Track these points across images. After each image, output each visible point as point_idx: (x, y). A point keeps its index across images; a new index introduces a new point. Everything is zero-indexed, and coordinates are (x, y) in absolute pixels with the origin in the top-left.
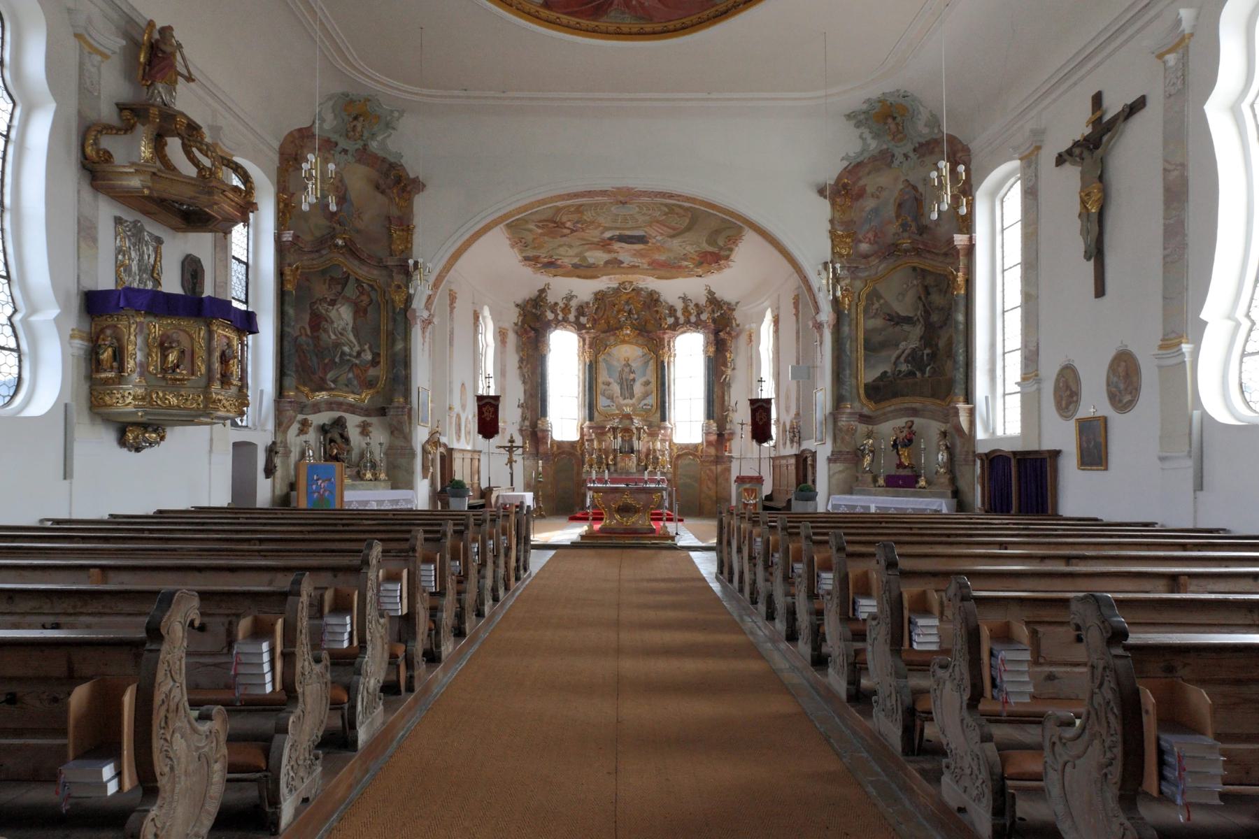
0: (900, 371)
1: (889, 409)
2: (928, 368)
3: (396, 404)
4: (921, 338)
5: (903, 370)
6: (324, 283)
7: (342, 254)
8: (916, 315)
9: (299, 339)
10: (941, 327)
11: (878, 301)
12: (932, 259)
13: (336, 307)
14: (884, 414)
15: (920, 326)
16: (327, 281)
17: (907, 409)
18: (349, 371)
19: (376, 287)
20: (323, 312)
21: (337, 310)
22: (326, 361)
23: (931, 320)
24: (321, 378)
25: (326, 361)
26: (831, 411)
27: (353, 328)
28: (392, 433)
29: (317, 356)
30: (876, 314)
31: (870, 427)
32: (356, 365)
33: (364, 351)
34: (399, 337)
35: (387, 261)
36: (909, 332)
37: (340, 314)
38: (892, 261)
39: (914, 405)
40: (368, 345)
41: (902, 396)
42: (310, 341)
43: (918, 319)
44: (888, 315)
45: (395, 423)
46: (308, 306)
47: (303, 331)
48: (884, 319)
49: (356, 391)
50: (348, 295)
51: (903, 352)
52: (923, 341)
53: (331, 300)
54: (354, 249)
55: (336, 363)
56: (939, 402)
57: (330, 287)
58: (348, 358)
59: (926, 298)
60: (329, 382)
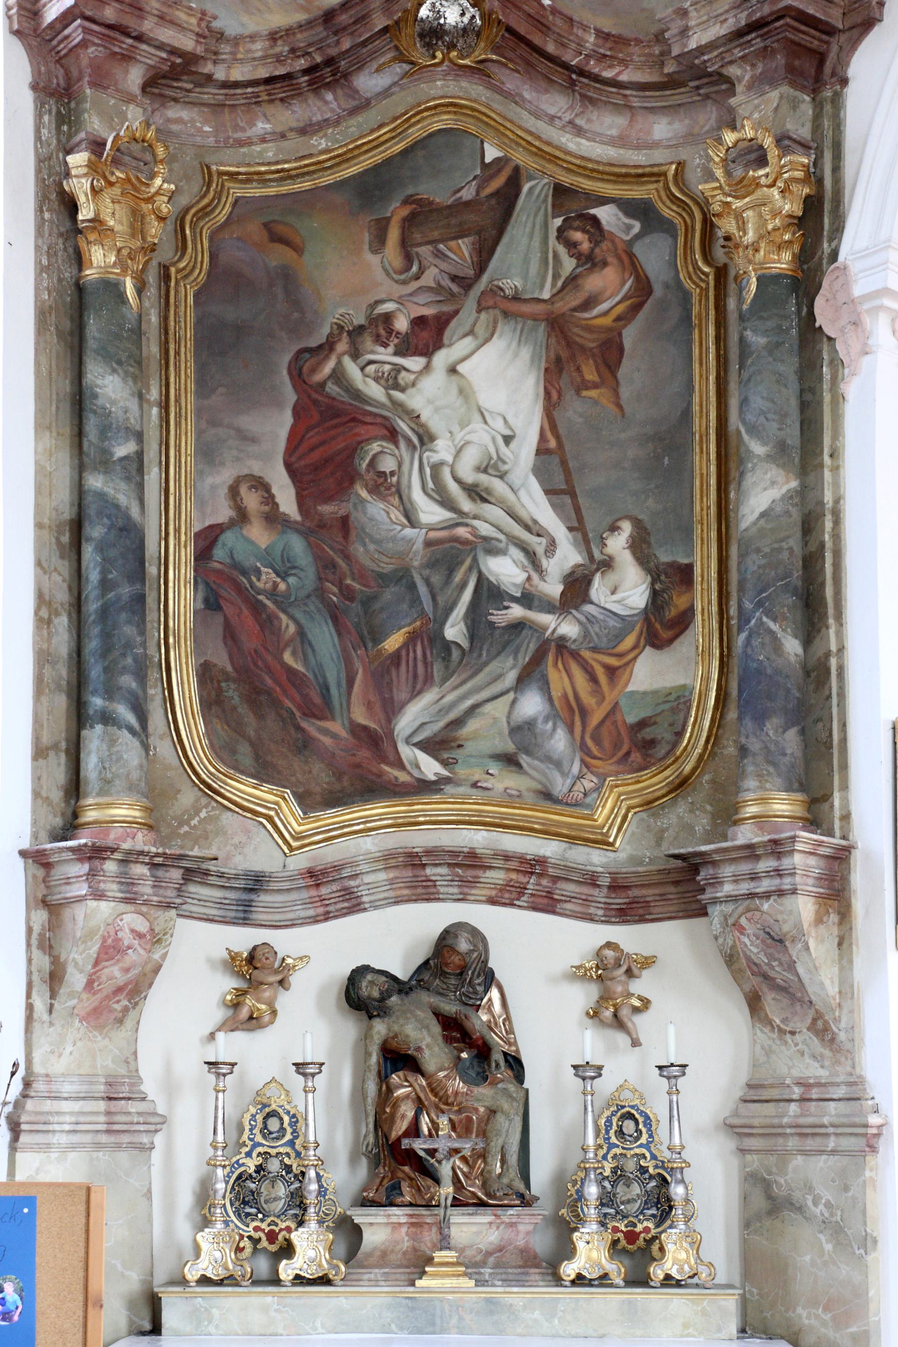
3: (745, 835)
6: (379, 241)
7: (480, 71)
9: (228, 538)
13: (441, 358)
16: (394, 234)
18: (521, 682)
19: (667, 211)
20: (375, 391)
21: (452, 371)
22: (393, 642)
24: (358, 731)
25: (393, 642)
27: (542, 451)
28: (754, 1003)
29: (336, 617)
32: (561, 645)
33: (607, 564)
34: (758, 448)
35: (684, 32)
37: (465, 392)
40: (627, 527)
42: (297, 545)
45: (751, 946)
46: (287, 358)
47: (251, 500)
49: (560, 786)
50: (511, 283)
53: (419, 322)
54: (522, 29)
55: (447, 646)
57: (409, 259)
58: (517, 611)
60: (406, 752)
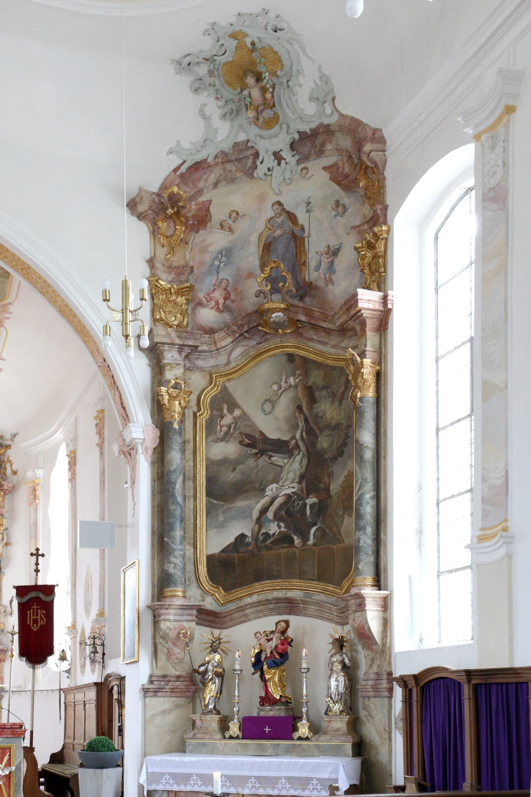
0: (267, 535)
1: (249, 600)
2: (313, 530)
4: (302, 477)
5: (271, 533)
8: (294, 437)
10: (334, 459)
11: (231, 411)
12: (321, 342)
14: (241, 609)
15: (298, 458)
17: (278, 600)
23: (319, 446)
26: (149, 603)
30: (227, 433)
31: (216, 632)
36: (281, 467)
38: (253, 342)
39: (290, 594)
41: (271, 577)
43: (297, 446)
44: (248, 436)
48: (241, 443)
51: (272, 503)
52: (304, 484)
56: (330, 587)
59: (311, 409)
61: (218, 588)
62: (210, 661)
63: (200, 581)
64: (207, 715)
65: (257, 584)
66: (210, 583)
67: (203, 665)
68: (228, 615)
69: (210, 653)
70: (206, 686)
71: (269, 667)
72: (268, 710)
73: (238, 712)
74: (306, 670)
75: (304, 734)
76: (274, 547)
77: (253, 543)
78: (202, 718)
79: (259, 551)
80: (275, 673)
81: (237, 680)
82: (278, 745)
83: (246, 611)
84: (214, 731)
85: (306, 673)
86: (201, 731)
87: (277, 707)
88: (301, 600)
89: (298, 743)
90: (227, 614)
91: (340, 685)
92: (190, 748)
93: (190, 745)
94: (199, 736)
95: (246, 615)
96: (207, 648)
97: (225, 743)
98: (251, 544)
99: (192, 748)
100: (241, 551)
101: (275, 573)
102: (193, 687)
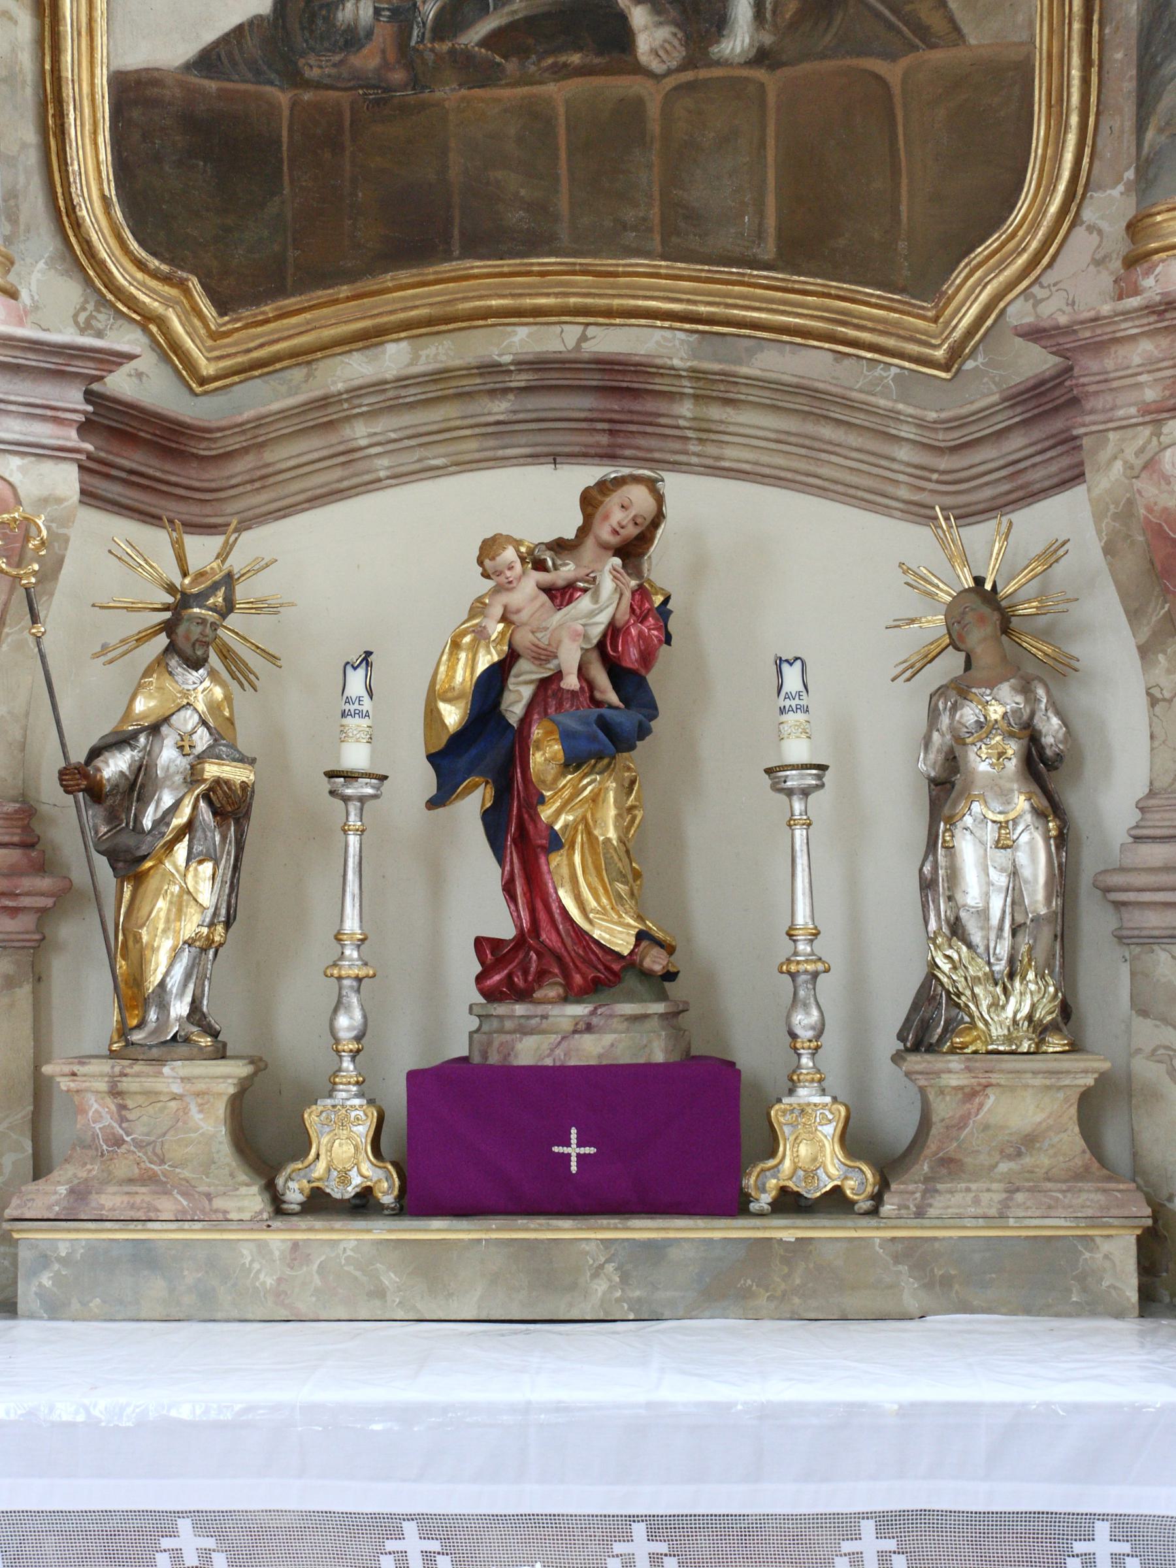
61: (182, 285)
62: (166, 720)
63: (77, 225)
64: (161, 1061)
65: (404, 276)
66: (134, 245)
67: (120, 741)
68: (245, 450)
69: (160, 664)
70: (139, 879)
71: (573, 762)
72: (567, 1025)
73: (358, 1039)
74: (809, 779)
75: (811, 1175)
76: (511, 66)
77: (384, 33)
78: (126, 1084)
79: (416, 83)
80: (595, 799)
81: (353, 840)
82: (654, 1250)
83: (347, 432)
84: (208, 1165)
85: (805, 793)
86: (123, 1168)
87: (629, 1008)
88: (696, 374)
89: (787, 1230)
90: (234, 443)
91: (1026, 872)
92: (46, 1280)
93: (44, 1261)
94: (110, 1200)
95: (349, 455)
96: (142, 638)
97: (296, 1245)
98: (369, 34)
99: (57, 1279)
100: (313, 73)
101: (515, 217)
102: (44, 883)
